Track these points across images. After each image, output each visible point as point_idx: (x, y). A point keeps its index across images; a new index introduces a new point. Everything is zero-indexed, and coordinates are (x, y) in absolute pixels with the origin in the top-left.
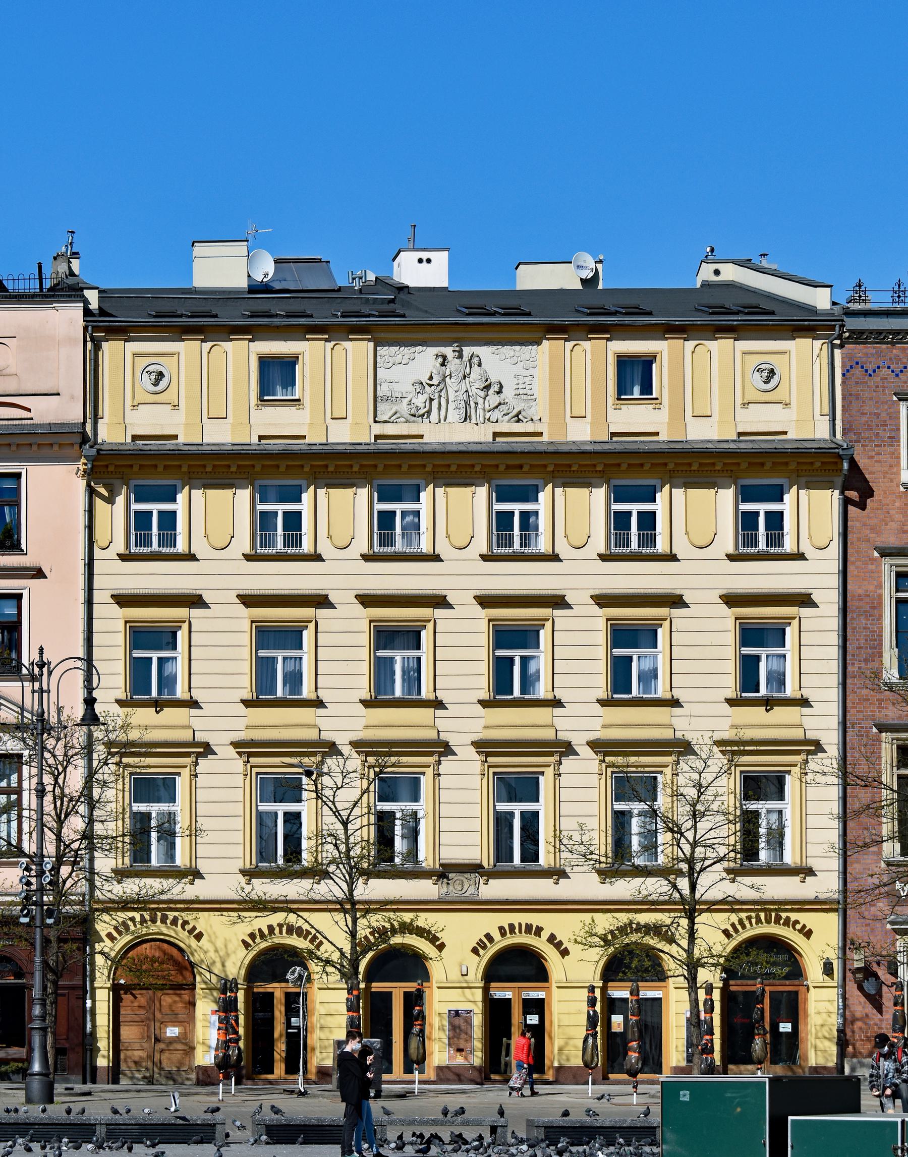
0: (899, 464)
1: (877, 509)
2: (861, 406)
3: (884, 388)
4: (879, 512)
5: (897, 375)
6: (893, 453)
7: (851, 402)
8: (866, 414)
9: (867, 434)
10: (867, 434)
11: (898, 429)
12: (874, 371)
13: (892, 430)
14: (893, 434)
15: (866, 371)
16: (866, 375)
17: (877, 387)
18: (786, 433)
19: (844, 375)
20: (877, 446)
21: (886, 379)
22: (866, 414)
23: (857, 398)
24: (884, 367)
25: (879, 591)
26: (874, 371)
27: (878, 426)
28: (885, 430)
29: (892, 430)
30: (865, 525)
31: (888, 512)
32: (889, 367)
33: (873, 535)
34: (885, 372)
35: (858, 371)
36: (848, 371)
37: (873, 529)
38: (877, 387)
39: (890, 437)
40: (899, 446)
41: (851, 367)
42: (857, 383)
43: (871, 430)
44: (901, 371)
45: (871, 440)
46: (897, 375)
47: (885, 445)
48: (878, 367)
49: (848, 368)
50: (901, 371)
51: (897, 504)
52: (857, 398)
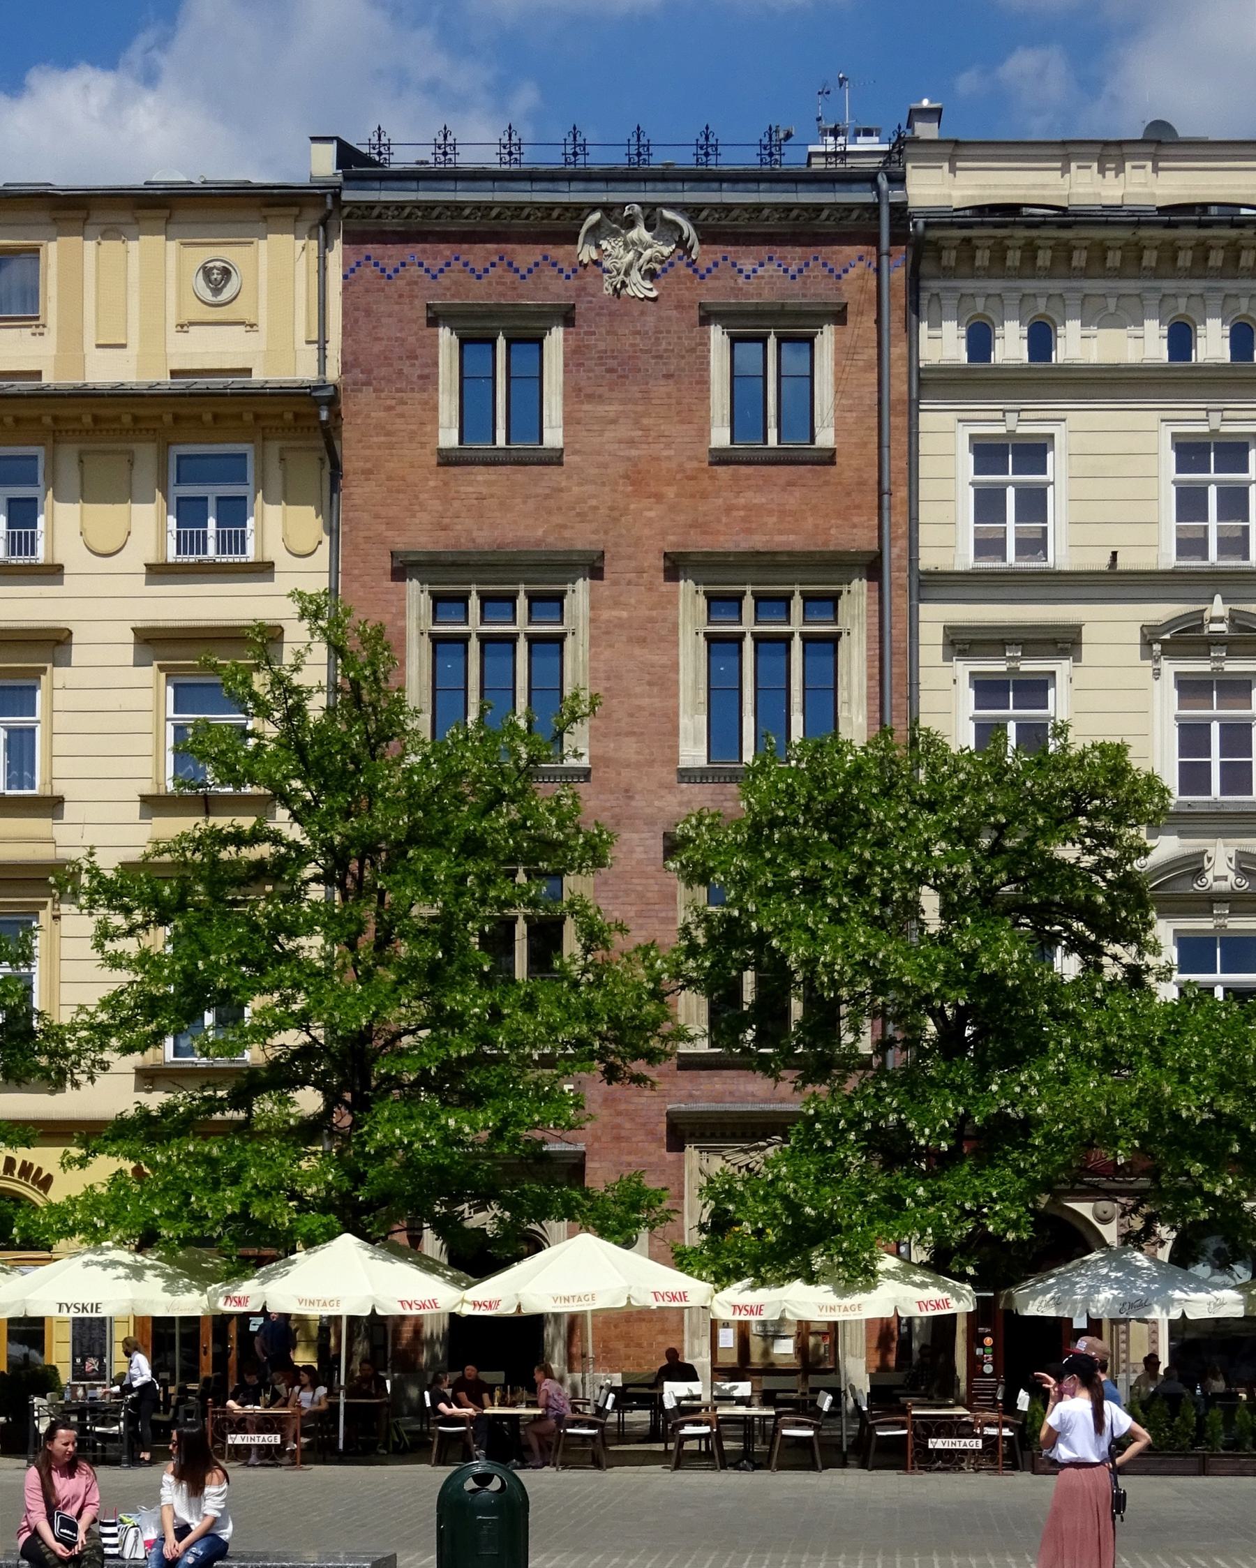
0: (435, 420)
1: (398, 491)
2: (374, 328)
3: (412, 297)
4: (401, 496)
5: (434, 277)
6: (426, 403)
7: (356, 321)
8: (381, 339)
9: (384, 371)
10: (384, 371)
11: (436, 364)
12: (396, 271)
13: (426, 365)
14: (426, 371)
15: (383, 270)
16: (382, 278)
17: (401, 296)
18: (248, 372)
19: (345, 277)
20: (399, 390)
21: (416, 283)
22: (381, 339)
23: (368, 312)
24: (412, 264)
25: (399, 623)
26: (396, 271)
27: (401, 358)
28: (413, 365)
29: (426, 365)
30: (377, 516)
31: (417, 497)
32: (421, 265)
33: (389, 533)
34: (415, 271)
35: (368, 272)
36: (353, 271)
37: (389, 523)
38: (401, 296)
39: (421, 377)
40: (437, 390)
41: (358, 264)
42: (367, 291)
43: (391, 365)
44: (441, 271)
45: (389, 381)
46: (434, 277)
47: (412, 390)
48: (403, 264)
49: (353, 265)
50: (441, 271)
51: (432, 483)
52: (368, 312)
